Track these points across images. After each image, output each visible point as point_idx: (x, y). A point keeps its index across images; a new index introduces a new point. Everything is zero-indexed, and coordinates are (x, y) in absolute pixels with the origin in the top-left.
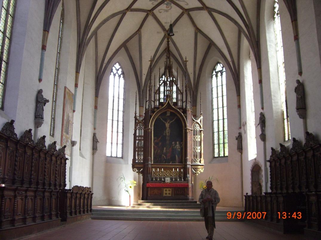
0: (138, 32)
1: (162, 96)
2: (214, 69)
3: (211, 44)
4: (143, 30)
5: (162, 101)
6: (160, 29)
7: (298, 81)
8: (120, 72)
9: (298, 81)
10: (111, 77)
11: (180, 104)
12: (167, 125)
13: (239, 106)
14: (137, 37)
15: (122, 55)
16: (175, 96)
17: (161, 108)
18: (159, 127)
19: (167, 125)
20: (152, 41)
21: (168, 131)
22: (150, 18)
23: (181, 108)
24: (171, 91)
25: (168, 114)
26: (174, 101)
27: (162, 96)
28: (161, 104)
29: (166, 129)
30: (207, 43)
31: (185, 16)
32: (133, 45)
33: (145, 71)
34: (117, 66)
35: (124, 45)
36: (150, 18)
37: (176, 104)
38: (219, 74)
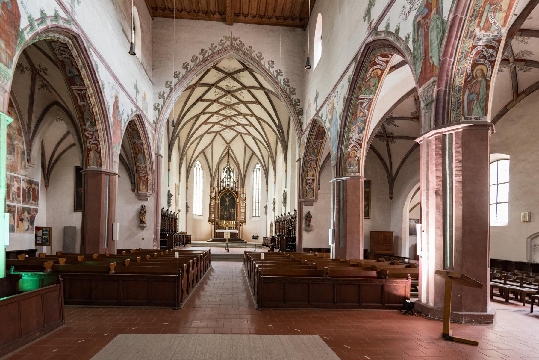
0: (211, 143)
1: (225, 184)
2: (255, 167)
3: (253, 153)
4: (213, 143)
5: (224, 187)
6: (224, 143)
7: (284, 191)
8: (200, 166)
9: (284, 191)
10: (195, 169)
11: (234, 189)
12: (227, 200)
13: (267, 190)
14: (210, 146)
15: (202, 157)
16: (232, 184)
17: (224, 191)
18: (223, 200)
19: (227, 200)
20: (219, 148)
21: (228, 203)
22: (218, 136)
23: (235, 191)
24: (230, 182)
25: (228, 194)
26: (232, 187)
27: (225, 184)
28: (224, 189)
29: (226, 202)
30: (251, 153)
31: (239, 136)
32: (208, 152)
33: (215, 167)
34: (198, 163)
35: (203, 152)
36: (218, 136)
37: (232, 189)
38: (258, 170)
